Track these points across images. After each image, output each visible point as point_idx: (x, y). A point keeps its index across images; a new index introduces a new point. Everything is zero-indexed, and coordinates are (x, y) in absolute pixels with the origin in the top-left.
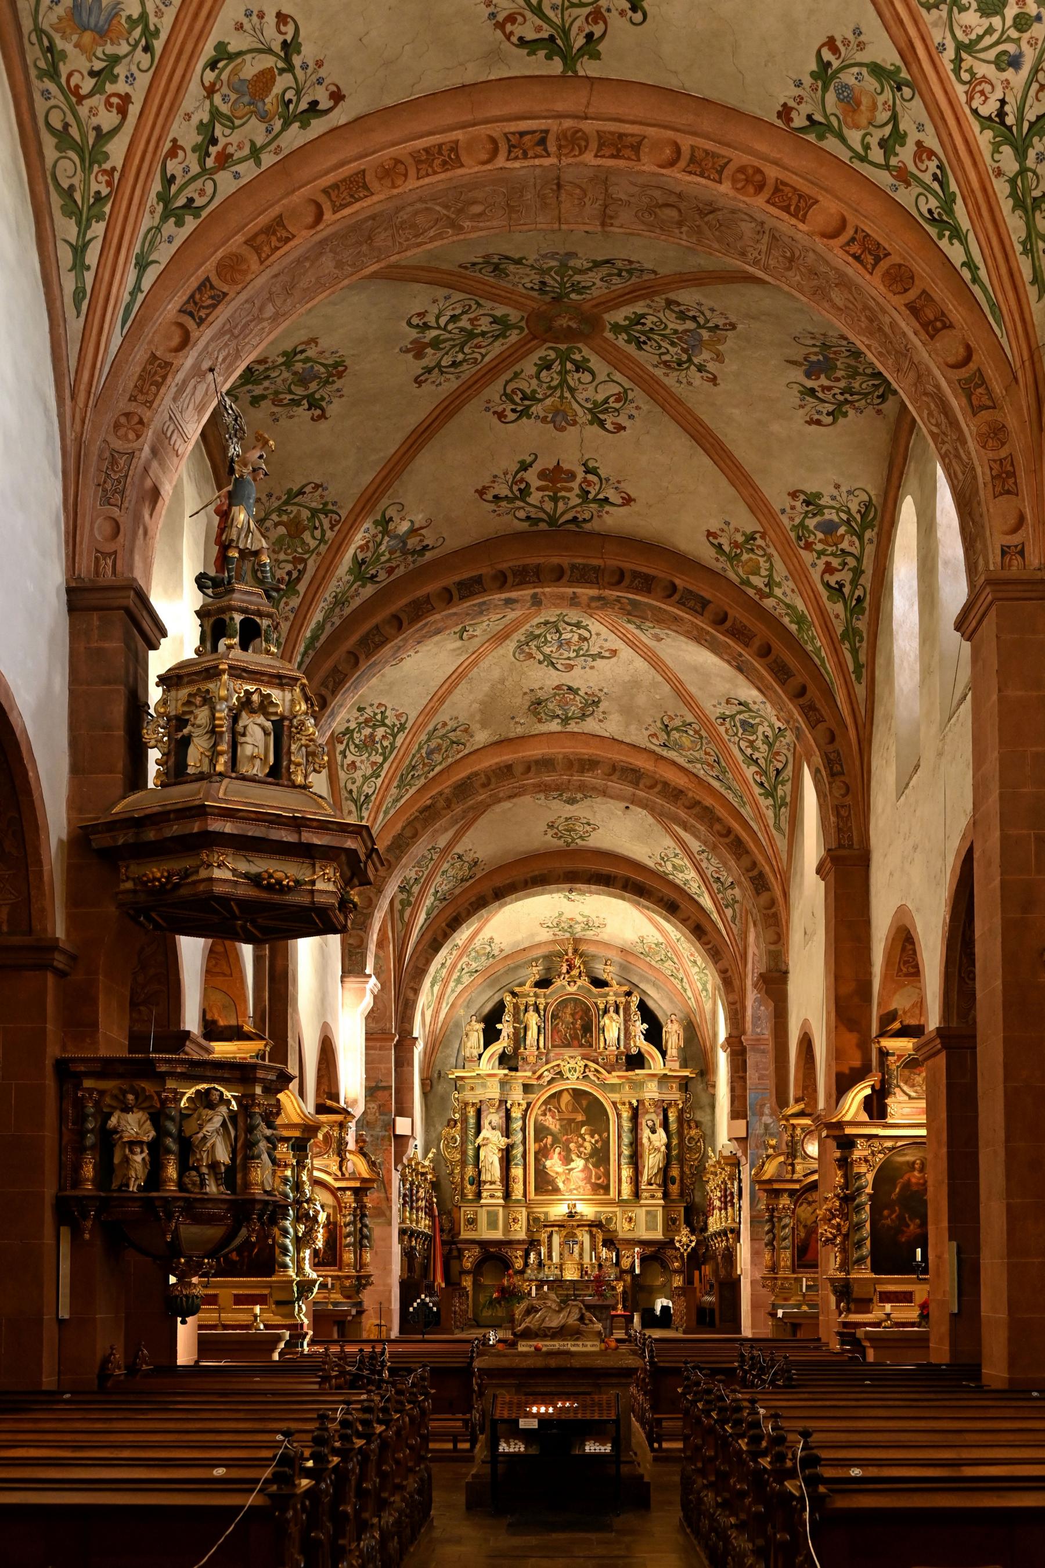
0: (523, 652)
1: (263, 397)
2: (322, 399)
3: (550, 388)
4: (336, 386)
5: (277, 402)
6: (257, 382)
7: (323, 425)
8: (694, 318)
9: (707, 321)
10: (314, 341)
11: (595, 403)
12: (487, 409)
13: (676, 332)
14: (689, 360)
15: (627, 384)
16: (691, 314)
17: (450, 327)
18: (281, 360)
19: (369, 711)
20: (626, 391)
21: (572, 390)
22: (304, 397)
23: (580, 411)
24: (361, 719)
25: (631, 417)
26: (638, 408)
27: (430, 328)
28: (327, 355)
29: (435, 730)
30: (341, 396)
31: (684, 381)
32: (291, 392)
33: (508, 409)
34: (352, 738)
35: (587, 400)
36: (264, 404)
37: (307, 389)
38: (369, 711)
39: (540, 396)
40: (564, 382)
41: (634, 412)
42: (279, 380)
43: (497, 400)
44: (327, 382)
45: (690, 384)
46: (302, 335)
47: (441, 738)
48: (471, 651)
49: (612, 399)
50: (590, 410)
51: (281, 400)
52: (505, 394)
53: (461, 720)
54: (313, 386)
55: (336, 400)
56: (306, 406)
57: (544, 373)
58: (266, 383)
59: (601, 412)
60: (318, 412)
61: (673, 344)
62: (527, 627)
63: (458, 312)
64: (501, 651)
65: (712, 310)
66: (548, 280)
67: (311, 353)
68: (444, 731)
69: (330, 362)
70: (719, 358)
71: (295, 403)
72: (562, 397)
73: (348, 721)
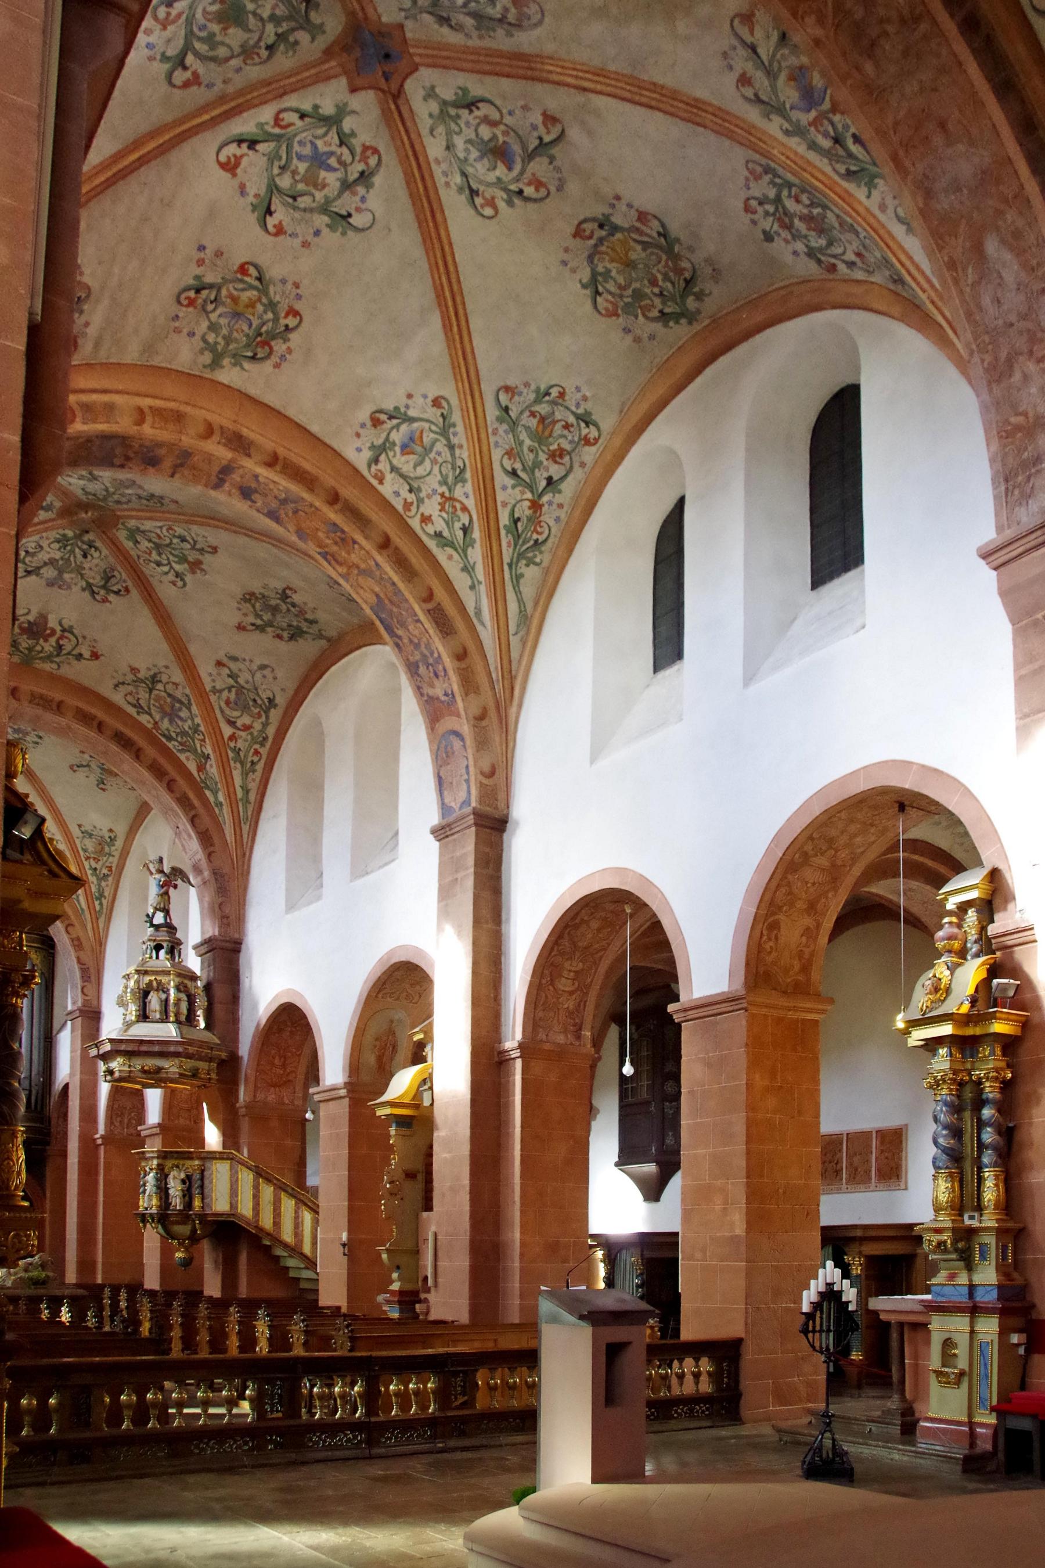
0: (522, 17)
1: (306, 620)
4: (262, 591)
6: (298, 628)
10: (240, 627)
18: (269, 629)
19: (767, 224)
22: (286, 603)
24: (785, 234)
28: (244, 611)
29: (758, 100)
32: (288, 610)
34: (821, 250)
37: (277, 605)
38: (767, 224)
42: (286, 620)
44: (264, 596)
46: (241, 637)
47: (771, 74)
48: (580, 98)
53: (727, 41)
54: (273, 602)
58: (295, 623)
60: (288, 591)
62: (475, 42)
64: (549, 48)
67: (251, 619)
68: (760, 78)
69: (248, 605)
71: (294, 605)
73: (795, 253)
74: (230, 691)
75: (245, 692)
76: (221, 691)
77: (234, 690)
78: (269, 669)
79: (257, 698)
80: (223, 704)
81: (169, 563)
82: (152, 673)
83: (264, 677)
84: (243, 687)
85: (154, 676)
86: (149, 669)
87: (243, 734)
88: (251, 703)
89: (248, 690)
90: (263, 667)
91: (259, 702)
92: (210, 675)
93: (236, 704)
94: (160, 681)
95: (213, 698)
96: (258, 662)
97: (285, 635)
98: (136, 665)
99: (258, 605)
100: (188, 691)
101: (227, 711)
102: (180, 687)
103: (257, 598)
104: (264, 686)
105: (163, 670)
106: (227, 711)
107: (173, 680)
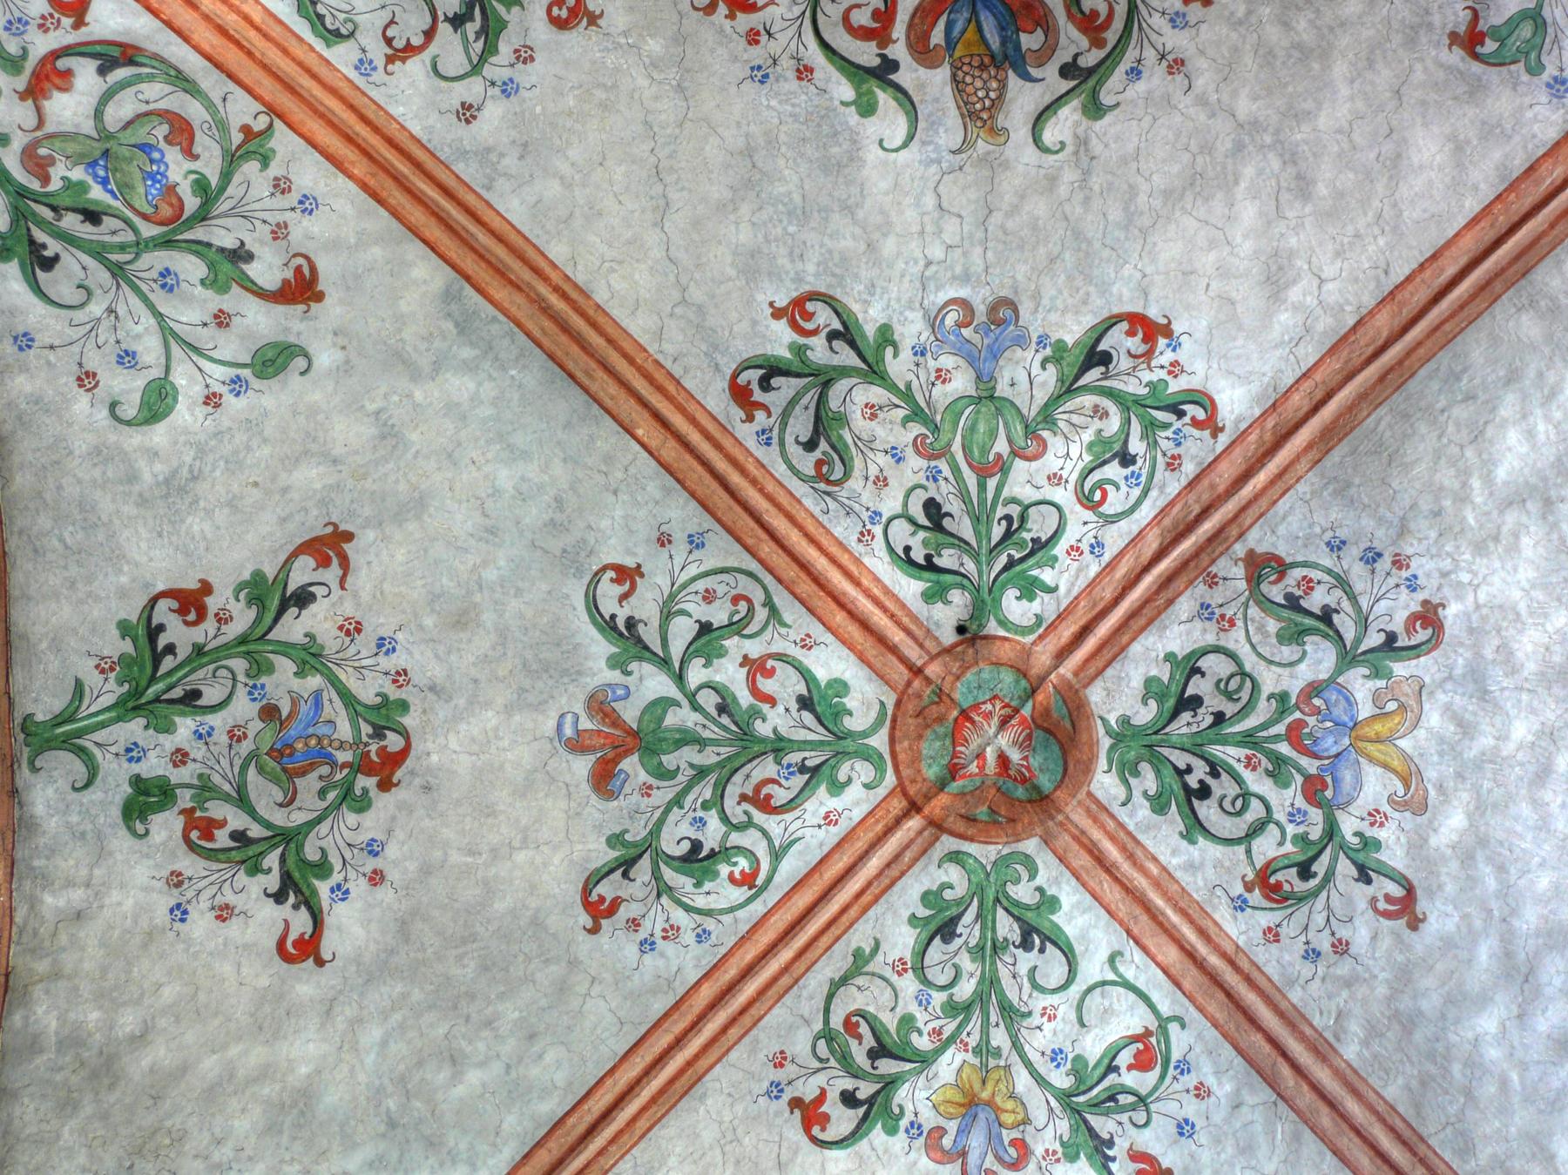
2: (322, 868)
3: (952, 1008)
4: (370, 824)
5: (199, 829)
7: (306, 984)
8: (1326, 616)
9: (1364, 623)
11: (1079, 1068)
12: (775, 1091)
13: (1282, 697)
14: (1331, 831)
15: (1166, 1000)
16: (1317, 600)
17: (697, 674)
18: (243, 619)
20: (1163, 1023)
21: (1012, 1015)
23: (1038, 1104)
25: (1184, 1128)
26: (1201, 1092)
27: (642, 649)
28: (365, 644)
30: (376, 878)
31: (1324, 943)
32: (242, 800)
33: (833, 1095)
35: (1056, 1056)
36: (166, 826)
39: (923, 1043)
40: (990, 983)
41: (1191, 1109)
43: (800, 1045)
45: (1341, 948)
49: (1125, 1058)
50: (1065, 1097)
51: (208, 828)
52: (828, 1035)
55: (358, 886)
56: (273, 881)
57: (936, 951)
58: (185, 726)
59: (1095, 1105)
60: (301, 923)
61: (1278, 770)
63: (719, 614)
65: (1371, 557)
66: (945, 493)
69: (367, 692)
70: (1413, 797)
72: (984, 1049)
74: (201, 186)
75: (148, 230)
76: (232, 160)
77: (191, 203)
78: (129, 411)
79: (85, 230)
80: (194, 111)
81: (692, 698)
82: (505, 49)
83: (127, 358)
84: (167, 243)
85: (491, 32)
86: (524, 56)
87: (42, 44)
88: (97, 193)
89: (141, 246)
90: (158, 401)
91: (71, 222)
92: (307, 204)
93: (145, 148)
94: (457, 21)
95: (242, 110)
96: (186, 413)
97: (177, 632)
98: (576, 39)
99: (344, 730)
100: (342, 57)
101: (156, 93)
102: (378, 52)
103: (364, 766)
104: (96, 308)
105: (472, 90)
106: (156, 93)
107: (416, 67)
